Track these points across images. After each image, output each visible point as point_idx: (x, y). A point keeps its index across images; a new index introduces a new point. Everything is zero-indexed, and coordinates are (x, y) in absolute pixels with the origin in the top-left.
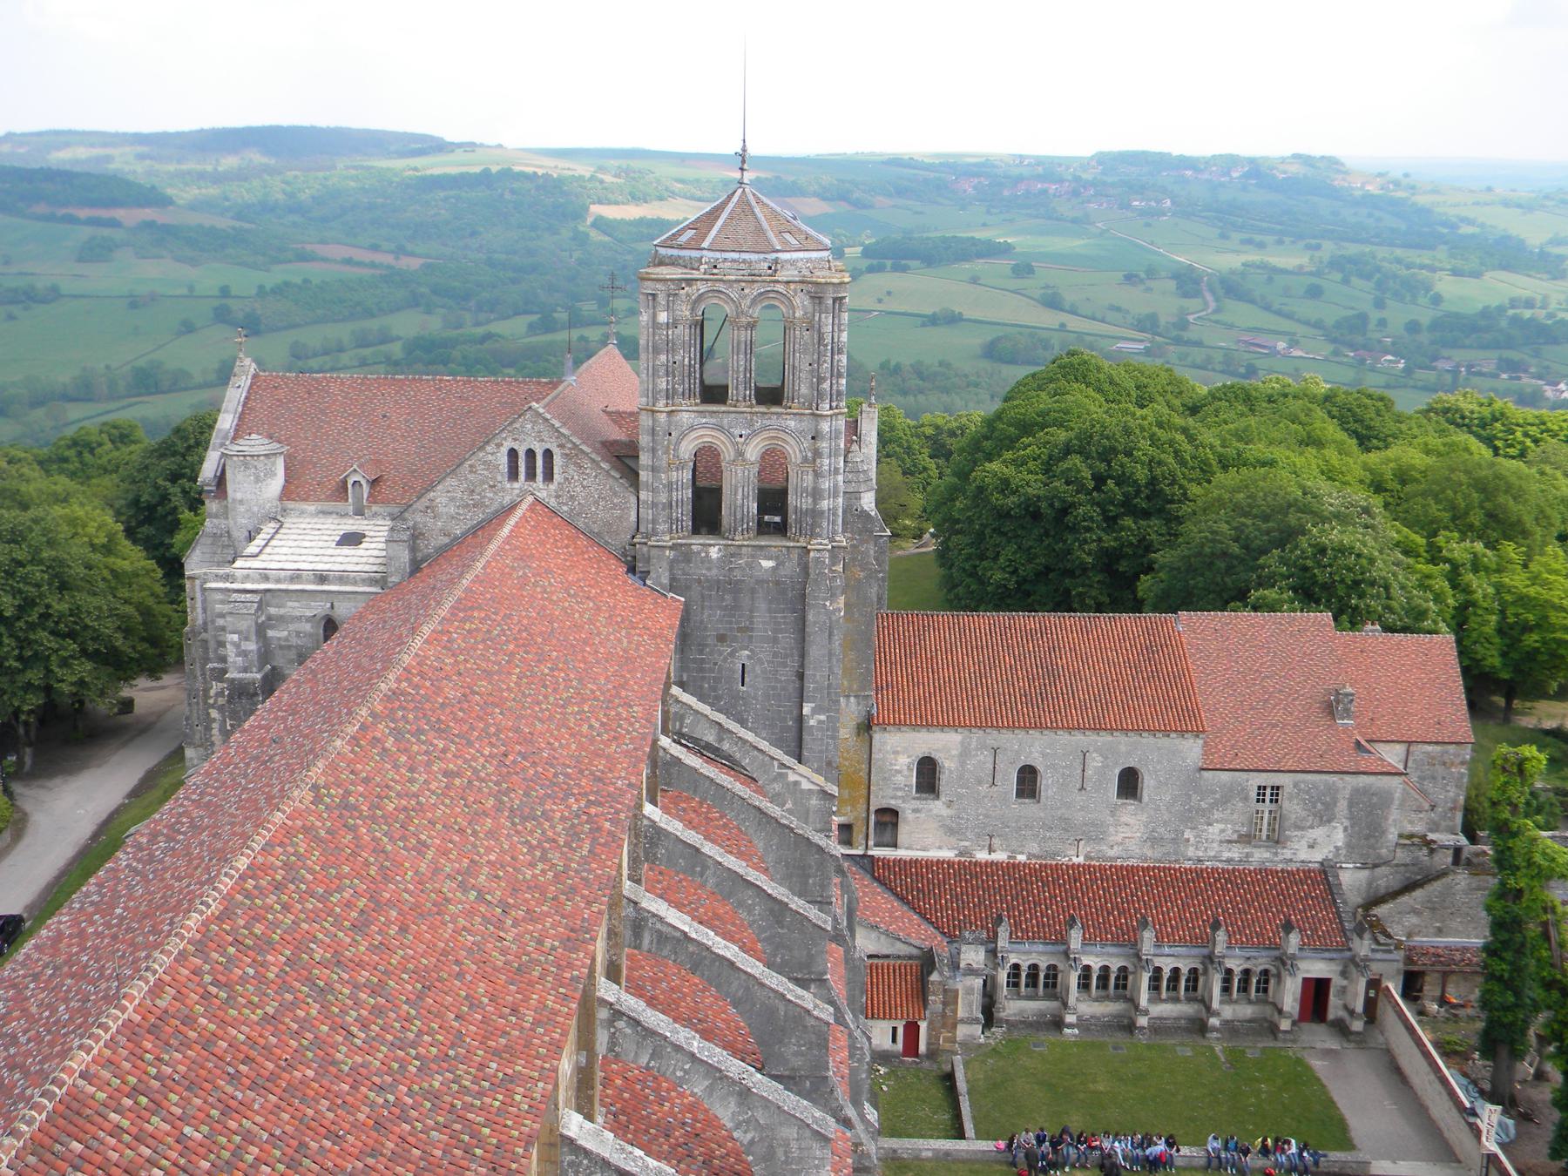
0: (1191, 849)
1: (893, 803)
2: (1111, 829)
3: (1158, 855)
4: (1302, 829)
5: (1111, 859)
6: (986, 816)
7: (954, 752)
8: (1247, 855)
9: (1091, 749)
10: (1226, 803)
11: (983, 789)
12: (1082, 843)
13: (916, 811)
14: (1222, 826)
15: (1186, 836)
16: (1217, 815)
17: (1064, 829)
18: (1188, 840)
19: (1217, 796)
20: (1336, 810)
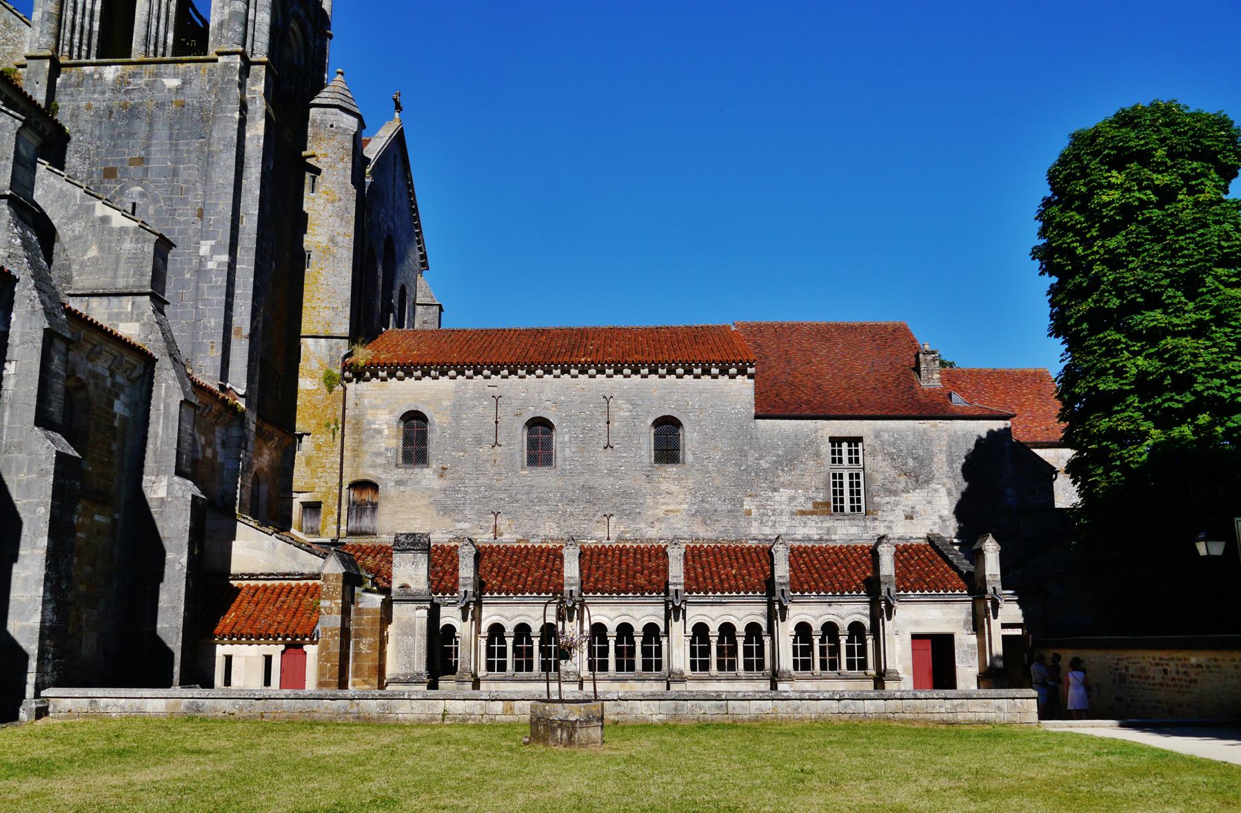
0: (755, 524)
1: (368, 474)
2: (649, 501)
3: (711, 535)
5: (650, 540)
6: (490, 488)
7: (446, 403)
9: (615, 395)
10: (791, 461)
11: (485, 450)
12: (613, 519)
13: (399, 483)
14: (792, 492)
15: (746, 507)
16: (783, 478)
17: (588, 502)
18: (749, 513)
19: (780, 452)
20: (934, 467)
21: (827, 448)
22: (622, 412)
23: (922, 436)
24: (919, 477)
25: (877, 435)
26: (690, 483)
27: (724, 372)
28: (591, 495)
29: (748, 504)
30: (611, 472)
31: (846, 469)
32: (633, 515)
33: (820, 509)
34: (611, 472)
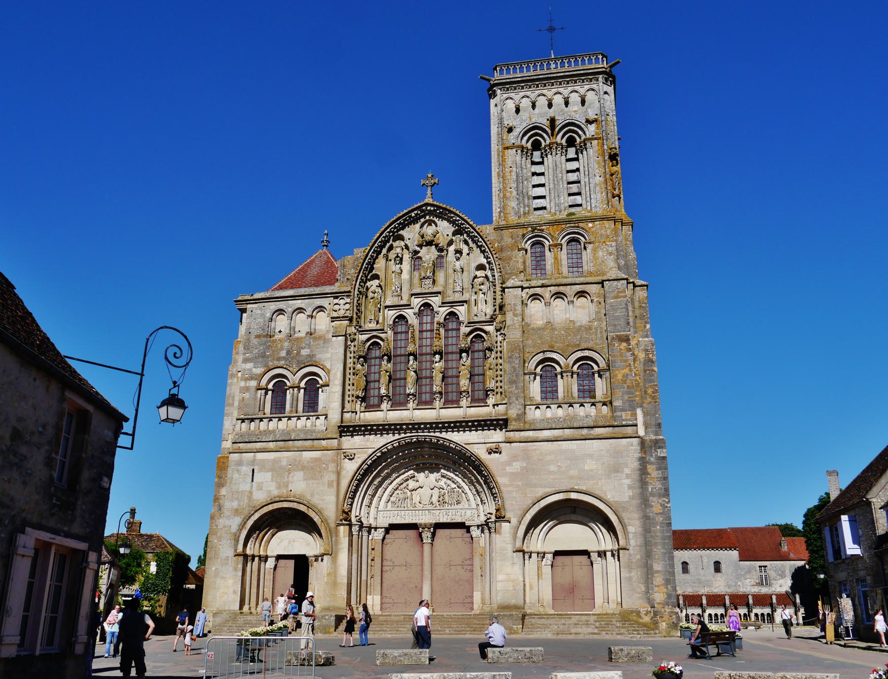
3: (731, 591)
4: (776, 580)
8: (760, 590)
16: (748, 576)
21: (758, 569)
22: (705, 560)
23: (783, 566)
24: (783, 576)
25: (771, 565)
26: (724, 578)
27: (730, 549)
28: (700, 581)
29: (739, 583)
30: (704, 575)
31: (763, 574)
32: (710, 586)
33: (758, 584)
34: (704, 575)
